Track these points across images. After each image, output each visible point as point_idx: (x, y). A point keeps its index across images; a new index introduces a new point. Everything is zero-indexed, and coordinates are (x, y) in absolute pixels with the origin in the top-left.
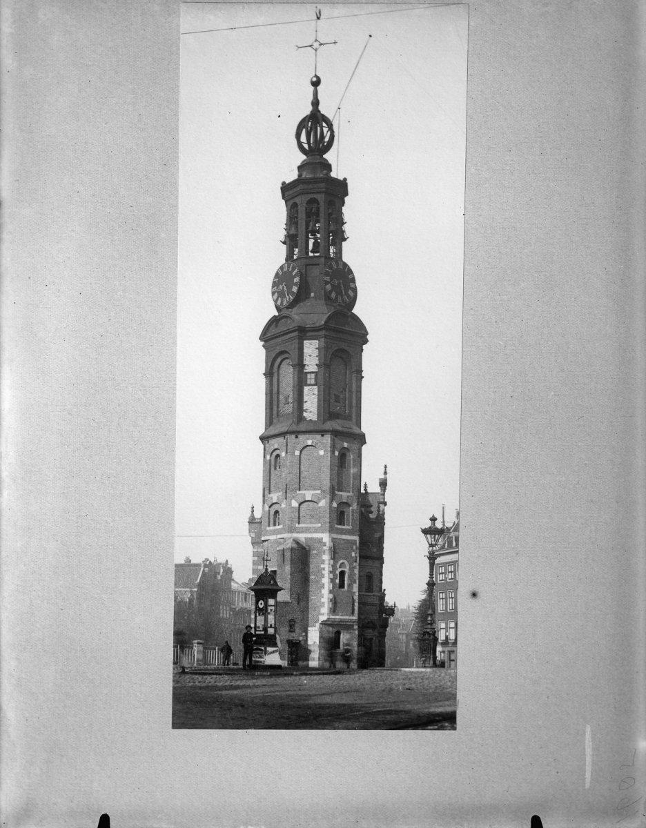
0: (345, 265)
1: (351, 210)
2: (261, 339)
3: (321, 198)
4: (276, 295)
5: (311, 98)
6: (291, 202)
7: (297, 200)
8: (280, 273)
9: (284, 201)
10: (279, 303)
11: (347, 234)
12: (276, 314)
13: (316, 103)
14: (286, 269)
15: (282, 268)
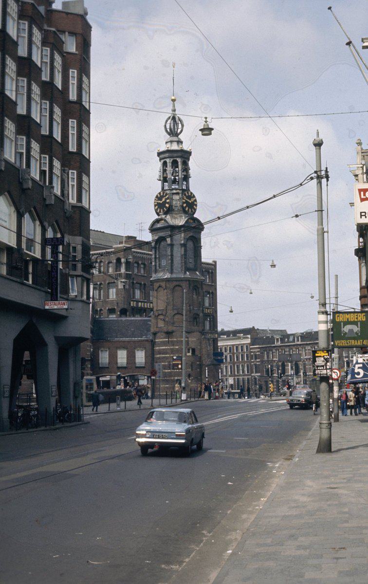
0: (191, 193)
1: (191, 163)
2: (149, 229)
3: (179, 160)
4: (157, 207)
5: (171, 108)
6: (162, 161)
7: (168, 160)
8: (159, 196)
9: (158, 158)
10: (158, 211)
11: (191, 175)
12: (157, 217)
13: (174, 110)
14: (162, 194)
15: (160, 193)
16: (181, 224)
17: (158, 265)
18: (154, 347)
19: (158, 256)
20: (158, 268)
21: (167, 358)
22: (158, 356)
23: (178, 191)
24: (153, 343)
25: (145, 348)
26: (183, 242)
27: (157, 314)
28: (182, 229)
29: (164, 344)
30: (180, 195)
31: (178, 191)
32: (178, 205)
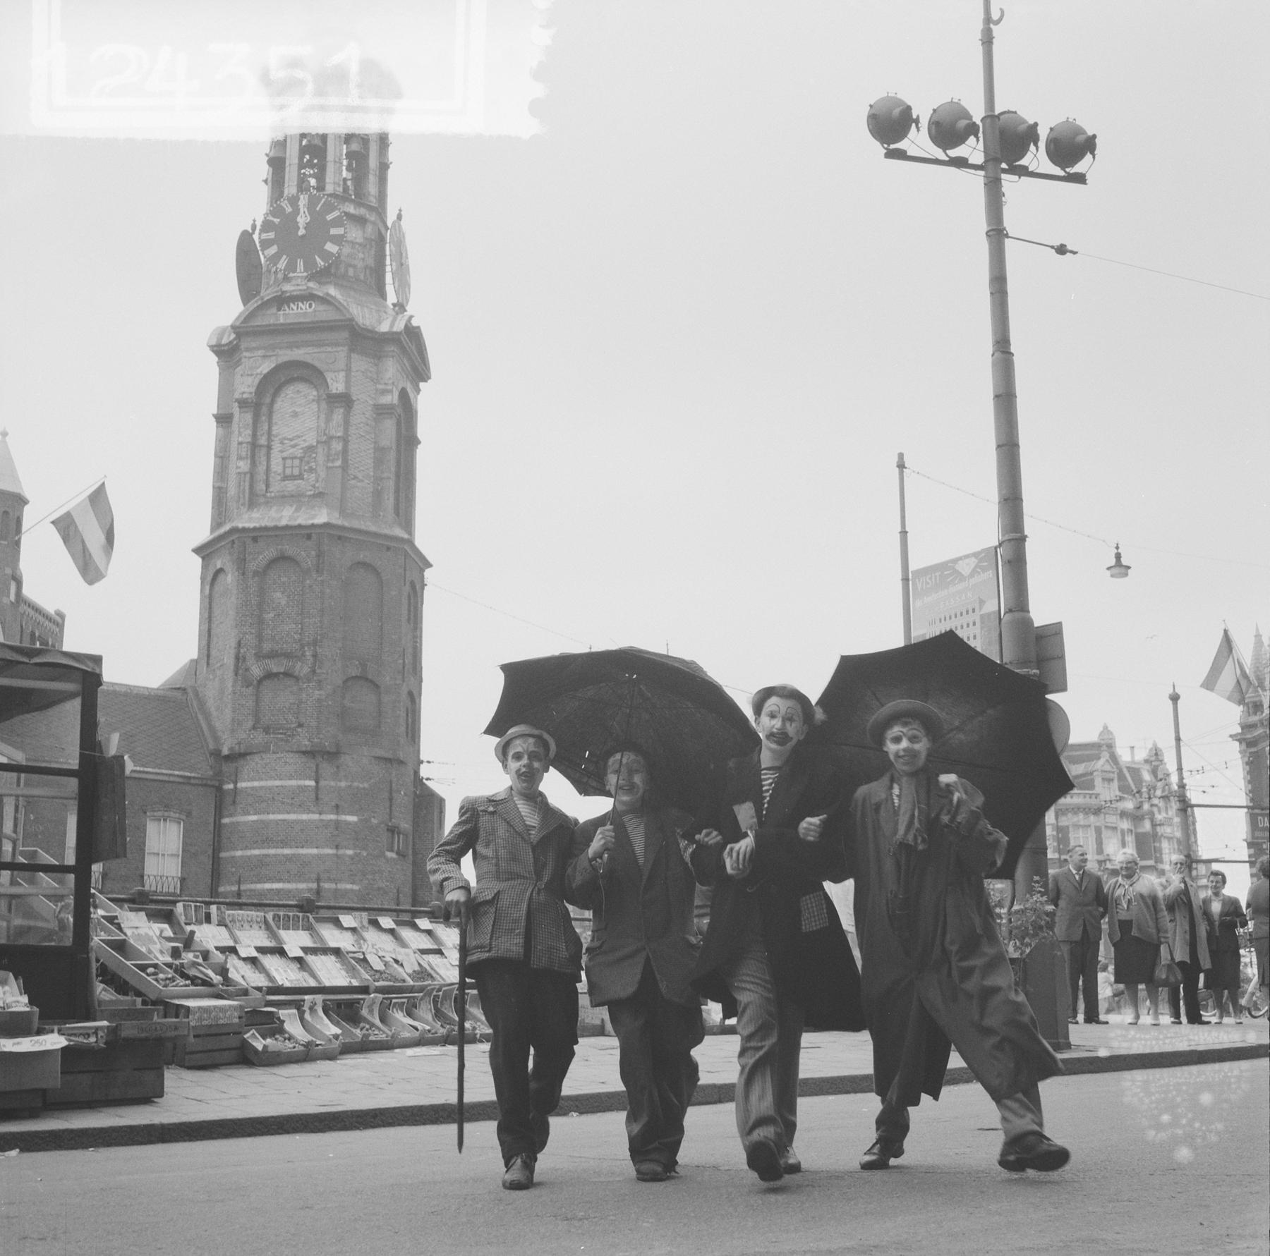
16: (384, 328)
17: (261, 475)
18: (221, 817)
19: (263, 441)
20: (261, 487)
21: (305, 862)
22: (256, 852)
23: (362, 211)
24: (222, 801)
25: (189, 814)
26: (387, 399)
27: (256, 671)
28: (391, 348)
29: (294, 800)
30: (369, 228)
31: (362, 211)
32: (360, 264)
